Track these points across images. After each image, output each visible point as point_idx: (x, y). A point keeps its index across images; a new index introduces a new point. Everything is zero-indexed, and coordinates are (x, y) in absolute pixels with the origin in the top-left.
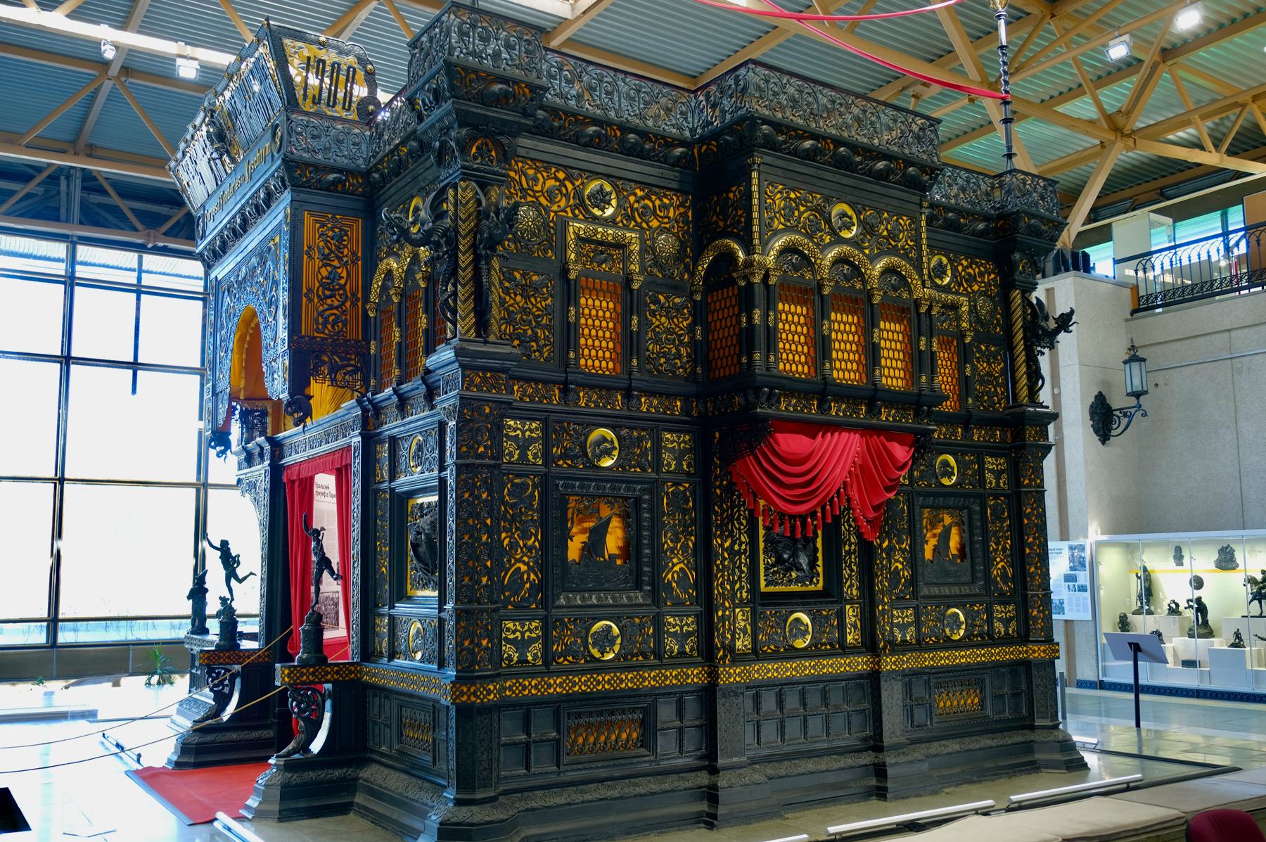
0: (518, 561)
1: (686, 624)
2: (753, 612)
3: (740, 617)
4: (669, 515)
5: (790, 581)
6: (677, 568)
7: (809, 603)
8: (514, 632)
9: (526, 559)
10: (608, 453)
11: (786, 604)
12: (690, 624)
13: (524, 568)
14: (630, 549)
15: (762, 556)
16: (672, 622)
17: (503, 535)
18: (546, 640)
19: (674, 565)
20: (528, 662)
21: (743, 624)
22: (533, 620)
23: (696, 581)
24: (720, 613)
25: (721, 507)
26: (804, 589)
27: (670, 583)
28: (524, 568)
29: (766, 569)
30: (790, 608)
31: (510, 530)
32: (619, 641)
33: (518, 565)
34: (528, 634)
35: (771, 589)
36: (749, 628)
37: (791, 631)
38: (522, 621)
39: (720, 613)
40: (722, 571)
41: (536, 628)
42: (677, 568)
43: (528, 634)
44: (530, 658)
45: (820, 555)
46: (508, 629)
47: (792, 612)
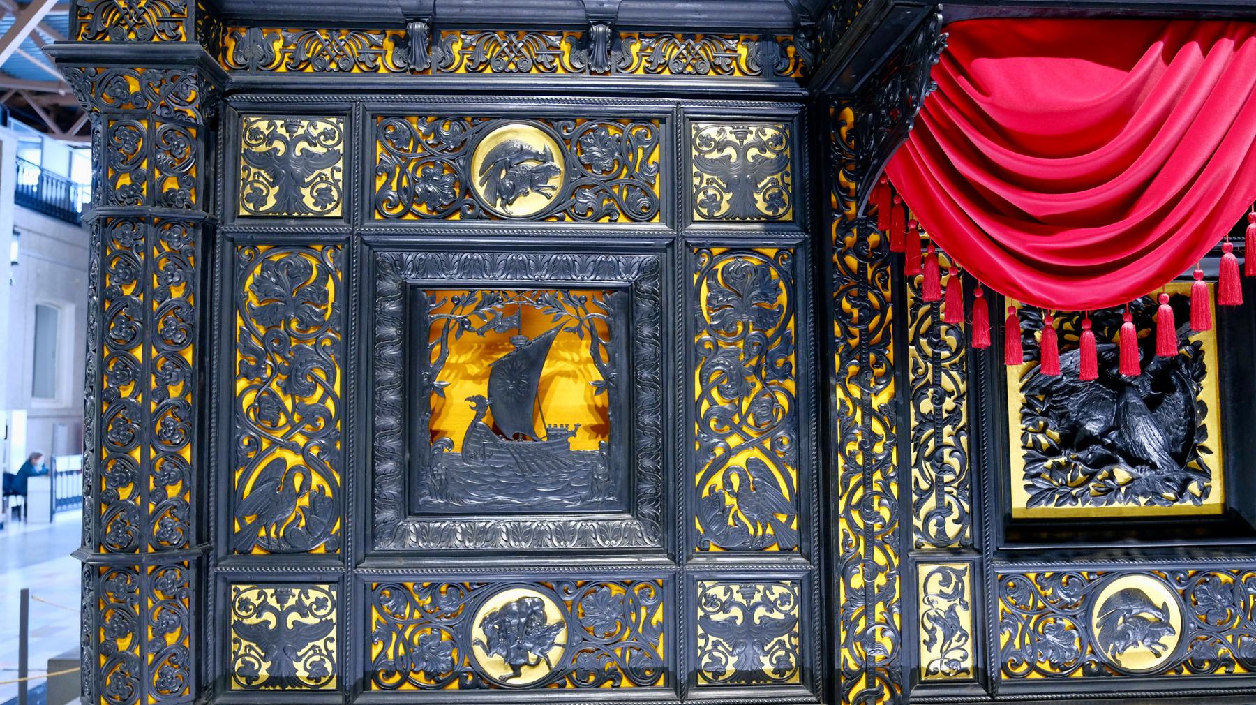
0: (274, 443)
1: (765, 602)
2: (980, 575)
3: (934, 586)
4: (713, 330)
5: (1109, 492)
6: (739, 461)
7: (1170, 554)
8: (259, 611)
9: (300, 440)
10: (534, 181)
11: (1091, 555)
12: (779, 601)
13: (292, 459)
14: (619, 415)
15: (1016, 427)
16: (722, 599)
17: (241, 384)
18: (353, 633)
19: (729, 452)
20: (296, 681)
21: (943, 605)
22: (313, 583)
23: (797, 497)
24: (857, 582)
25: (860, 302)
26: (1158, 509)
27: (716, 499)
28: (292, 459)
29: (1030, 461)
30: (1103, 565)
31: (258, 370)
32: (561, 637)
33: (279, 453)
34: (294, 616)
35: (1048, 509)
36: (965, 619)
37: (1108, 622)
38: (282, 584)
39: (857, 582)
40: (867, 471)
41: (320, 604)
42: (739, 461)
43: (294, 616)
44: (302, 674)
45: (1211, 422)
46: (245, 604)
47: (1109, 577)
